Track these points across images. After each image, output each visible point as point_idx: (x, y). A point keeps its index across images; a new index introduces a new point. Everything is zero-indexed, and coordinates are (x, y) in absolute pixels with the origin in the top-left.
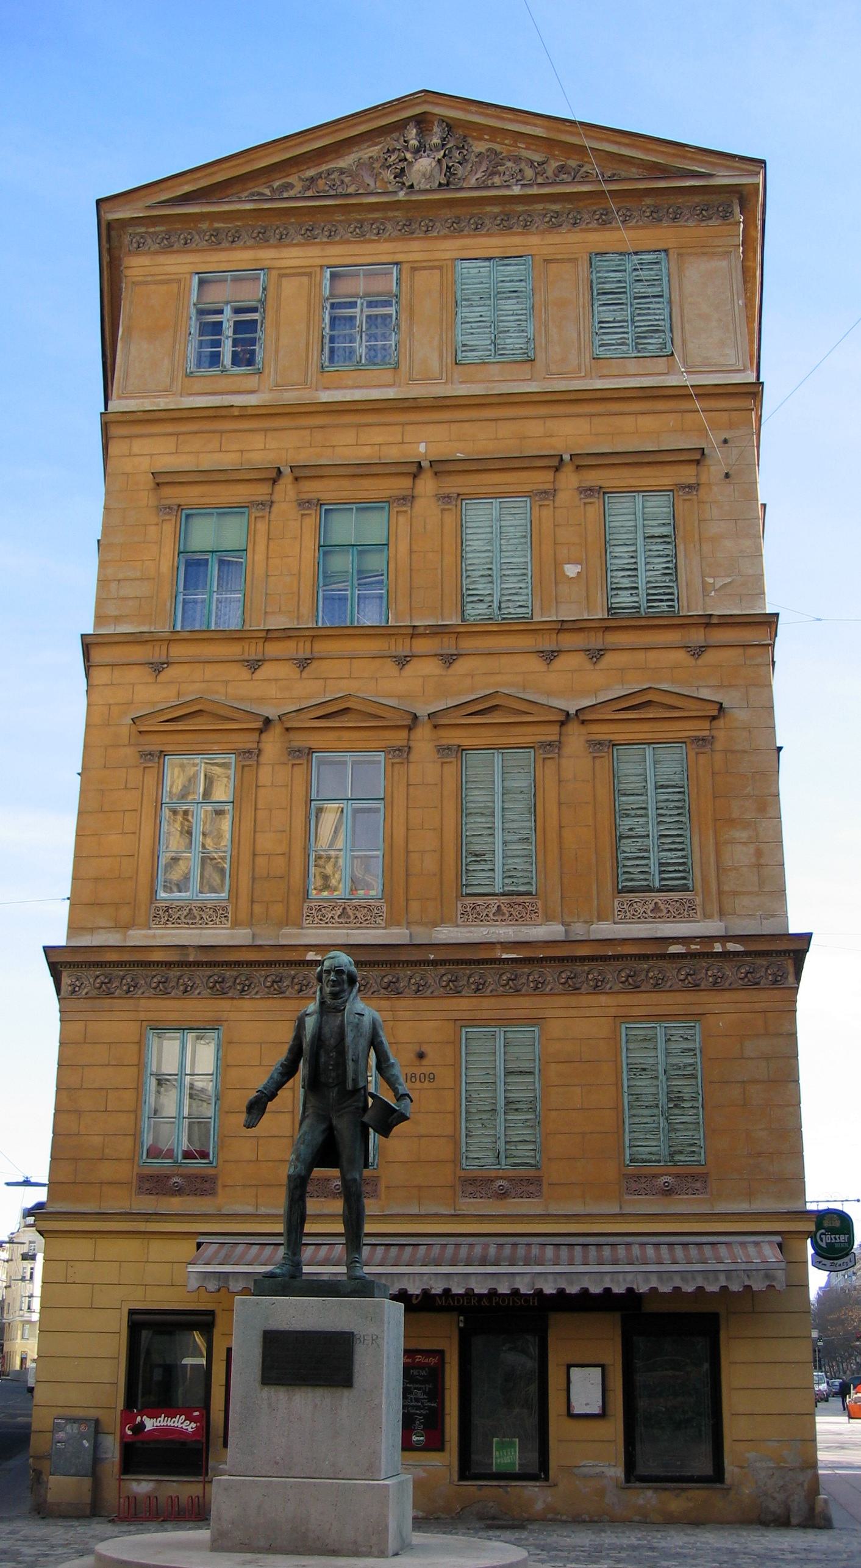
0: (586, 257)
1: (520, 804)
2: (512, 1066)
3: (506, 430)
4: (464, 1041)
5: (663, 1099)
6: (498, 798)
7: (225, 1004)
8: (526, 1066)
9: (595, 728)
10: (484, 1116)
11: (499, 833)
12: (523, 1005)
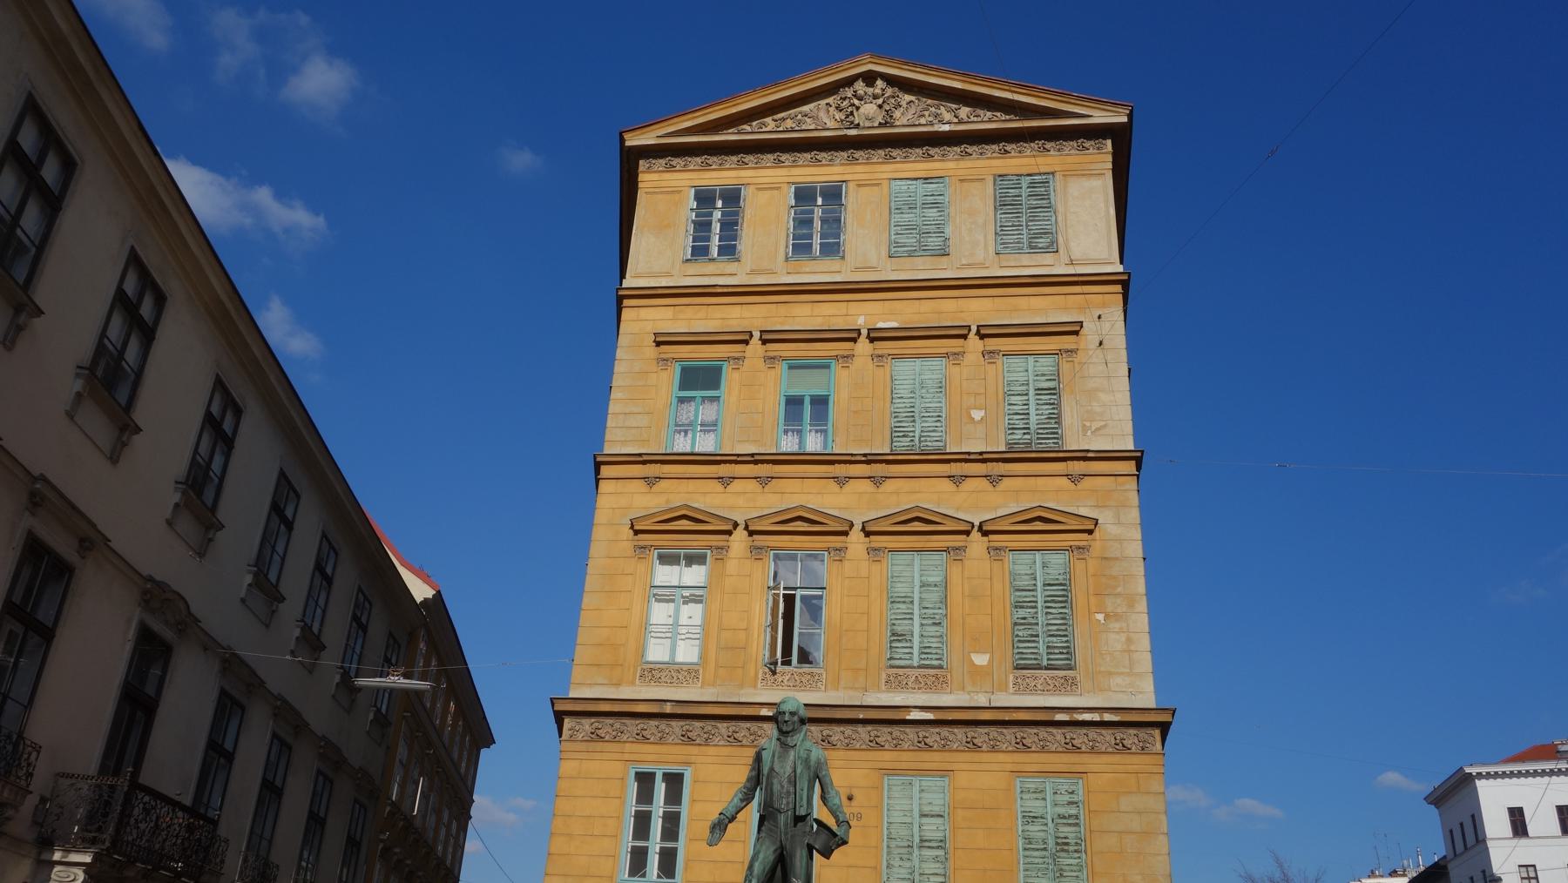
1: (933, 596)
2: (926, 809)
5: (1051, 843)
6: (917, 589)
7: (694, 750)
8: (936, 810)
9: (992, 537)
11: (916, 617)
12: (934, 759)
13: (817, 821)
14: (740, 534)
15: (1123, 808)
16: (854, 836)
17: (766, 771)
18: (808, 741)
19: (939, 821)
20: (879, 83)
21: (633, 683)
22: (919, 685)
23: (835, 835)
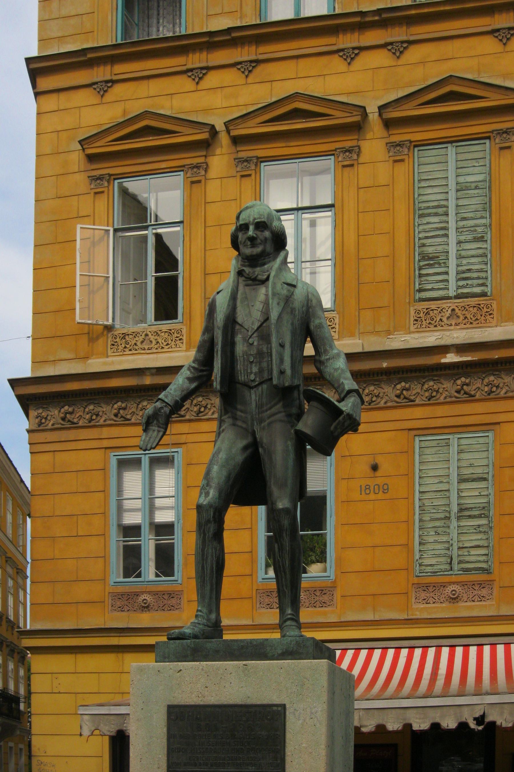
4: (417, 450)
10: (437, 524)
19: (482, 484)
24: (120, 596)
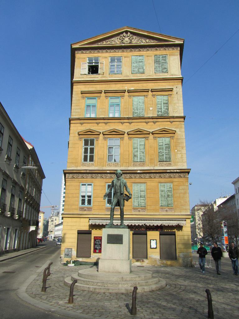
0: (154, 56)
1: (142, 147)
2: (141, 190)
3: (140, 85)
7: (94, 179)
9: (154, 135)
13: (125, 194)
14: (101, 135)
15: (180, 188)
16: (133, 197)
17: (115, 185)
18: (123, 179)
19: (144, 192)
20: (129, 33)
21: (80, 166)
22: (140, 165)
23: (129, 197)
24: (81, 208)
